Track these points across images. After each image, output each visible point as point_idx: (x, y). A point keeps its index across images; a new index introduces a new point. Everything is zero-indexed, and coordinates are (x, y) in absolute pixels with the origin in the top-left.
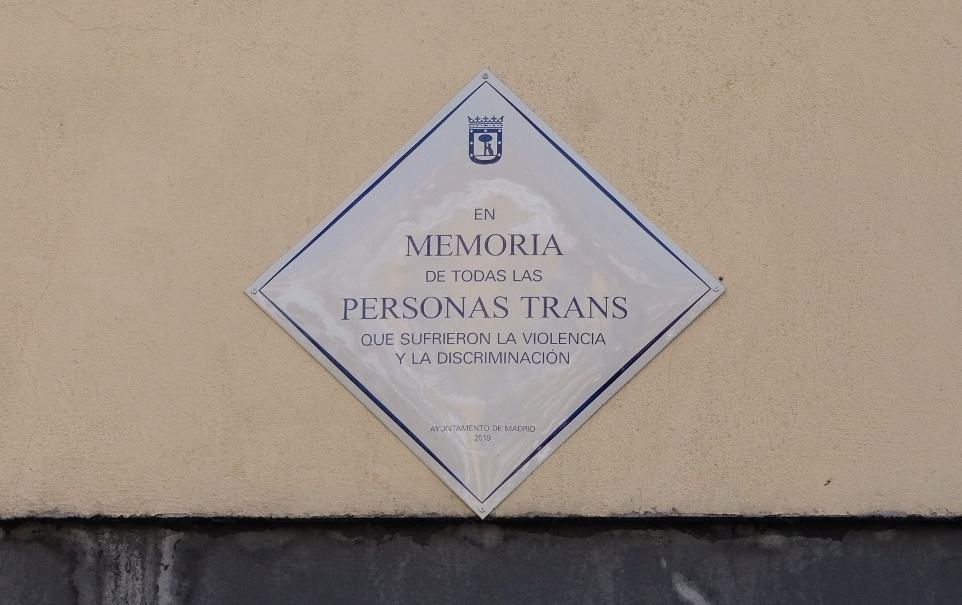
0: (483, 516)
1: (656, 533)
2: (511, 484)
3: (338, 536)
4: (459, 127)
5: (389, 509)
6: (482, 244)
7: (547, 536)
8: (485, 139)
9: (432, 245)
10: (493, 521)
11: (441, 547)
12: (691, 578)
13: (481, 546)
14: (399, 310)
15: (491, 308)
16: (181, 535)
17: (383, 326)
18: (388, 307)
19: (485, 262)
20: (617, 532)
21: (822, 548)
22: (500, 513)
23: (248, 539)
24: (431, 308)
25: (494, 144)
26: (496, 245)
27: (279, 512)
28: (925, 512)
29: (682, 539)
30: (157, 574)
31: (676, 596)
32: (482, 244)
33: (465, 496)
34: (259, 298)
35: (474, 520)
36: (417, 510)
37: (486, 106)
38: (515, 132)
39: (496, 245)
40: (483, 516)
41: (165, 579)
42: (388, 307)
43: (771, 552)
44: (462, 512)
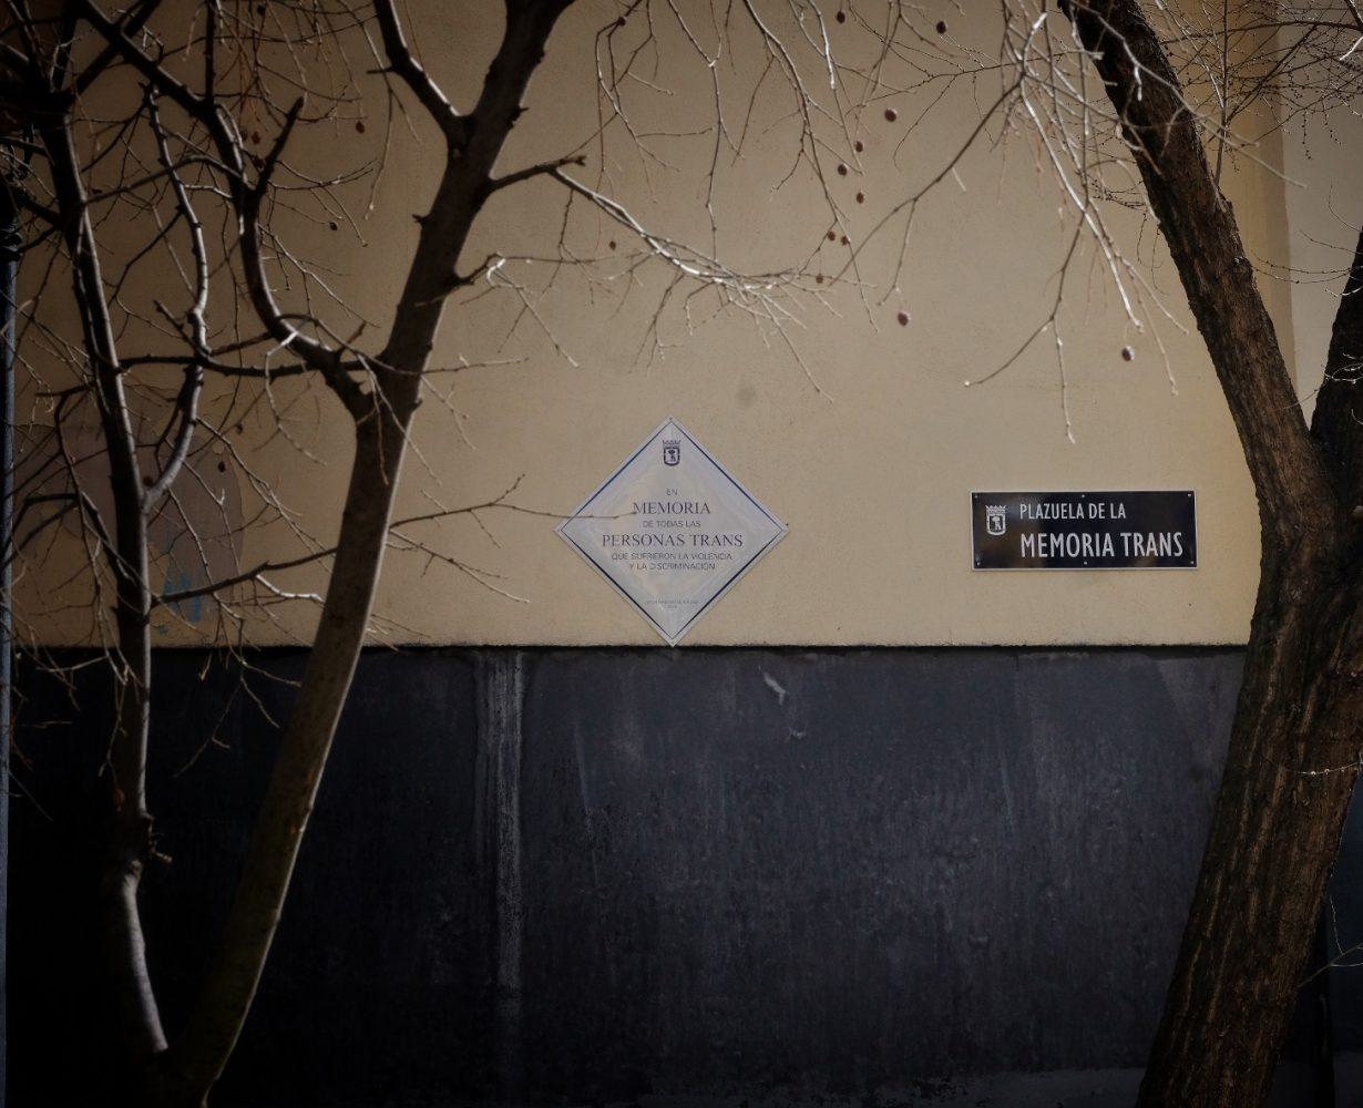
0: (673, 646)
1: (756, 653)
2: (684, 632)
3: (601, 654)
4: (657, 447)
5: (627, 642)
6: (671, 507)
7: (703, 654)
8: (670, 452)
9: (647, 508)
10: (677, 647)
11: (651, 659)
12: (772, 675)
13: (671, 659)
14: (631, 541)
15: (675, 540)
16: (526, 654)
17: (625, 549)
18: (625, 540)
19: (673, 517)
20: (737, 652)
21: (834, 659)
22: (681, 645)
23: (558, 655)
24: (646, 540)
25: (676, 455)
26: (678, 508)
27: (574, 644)
28: (885, 644)
29: (769, 656)
30: (514, 672)
31: (766, 685)
32: (671, 507)
33: (665, 636)
34: (560, 534)
35: (669, 647)
36: (640, 642)
37: (670, 434)
38: (686, 447)
39: (678, 508)
40: (673, 646)
41: (518, 676)
42: (625, 540)
43: (811, 662)
44: (663, 644)
